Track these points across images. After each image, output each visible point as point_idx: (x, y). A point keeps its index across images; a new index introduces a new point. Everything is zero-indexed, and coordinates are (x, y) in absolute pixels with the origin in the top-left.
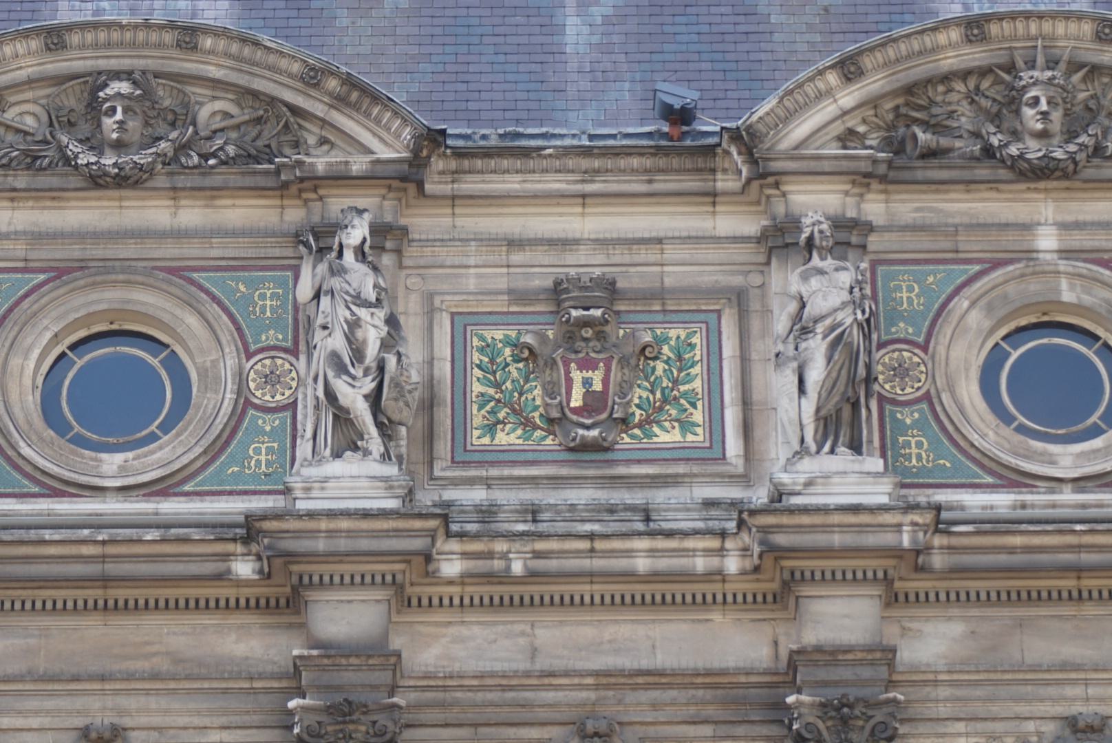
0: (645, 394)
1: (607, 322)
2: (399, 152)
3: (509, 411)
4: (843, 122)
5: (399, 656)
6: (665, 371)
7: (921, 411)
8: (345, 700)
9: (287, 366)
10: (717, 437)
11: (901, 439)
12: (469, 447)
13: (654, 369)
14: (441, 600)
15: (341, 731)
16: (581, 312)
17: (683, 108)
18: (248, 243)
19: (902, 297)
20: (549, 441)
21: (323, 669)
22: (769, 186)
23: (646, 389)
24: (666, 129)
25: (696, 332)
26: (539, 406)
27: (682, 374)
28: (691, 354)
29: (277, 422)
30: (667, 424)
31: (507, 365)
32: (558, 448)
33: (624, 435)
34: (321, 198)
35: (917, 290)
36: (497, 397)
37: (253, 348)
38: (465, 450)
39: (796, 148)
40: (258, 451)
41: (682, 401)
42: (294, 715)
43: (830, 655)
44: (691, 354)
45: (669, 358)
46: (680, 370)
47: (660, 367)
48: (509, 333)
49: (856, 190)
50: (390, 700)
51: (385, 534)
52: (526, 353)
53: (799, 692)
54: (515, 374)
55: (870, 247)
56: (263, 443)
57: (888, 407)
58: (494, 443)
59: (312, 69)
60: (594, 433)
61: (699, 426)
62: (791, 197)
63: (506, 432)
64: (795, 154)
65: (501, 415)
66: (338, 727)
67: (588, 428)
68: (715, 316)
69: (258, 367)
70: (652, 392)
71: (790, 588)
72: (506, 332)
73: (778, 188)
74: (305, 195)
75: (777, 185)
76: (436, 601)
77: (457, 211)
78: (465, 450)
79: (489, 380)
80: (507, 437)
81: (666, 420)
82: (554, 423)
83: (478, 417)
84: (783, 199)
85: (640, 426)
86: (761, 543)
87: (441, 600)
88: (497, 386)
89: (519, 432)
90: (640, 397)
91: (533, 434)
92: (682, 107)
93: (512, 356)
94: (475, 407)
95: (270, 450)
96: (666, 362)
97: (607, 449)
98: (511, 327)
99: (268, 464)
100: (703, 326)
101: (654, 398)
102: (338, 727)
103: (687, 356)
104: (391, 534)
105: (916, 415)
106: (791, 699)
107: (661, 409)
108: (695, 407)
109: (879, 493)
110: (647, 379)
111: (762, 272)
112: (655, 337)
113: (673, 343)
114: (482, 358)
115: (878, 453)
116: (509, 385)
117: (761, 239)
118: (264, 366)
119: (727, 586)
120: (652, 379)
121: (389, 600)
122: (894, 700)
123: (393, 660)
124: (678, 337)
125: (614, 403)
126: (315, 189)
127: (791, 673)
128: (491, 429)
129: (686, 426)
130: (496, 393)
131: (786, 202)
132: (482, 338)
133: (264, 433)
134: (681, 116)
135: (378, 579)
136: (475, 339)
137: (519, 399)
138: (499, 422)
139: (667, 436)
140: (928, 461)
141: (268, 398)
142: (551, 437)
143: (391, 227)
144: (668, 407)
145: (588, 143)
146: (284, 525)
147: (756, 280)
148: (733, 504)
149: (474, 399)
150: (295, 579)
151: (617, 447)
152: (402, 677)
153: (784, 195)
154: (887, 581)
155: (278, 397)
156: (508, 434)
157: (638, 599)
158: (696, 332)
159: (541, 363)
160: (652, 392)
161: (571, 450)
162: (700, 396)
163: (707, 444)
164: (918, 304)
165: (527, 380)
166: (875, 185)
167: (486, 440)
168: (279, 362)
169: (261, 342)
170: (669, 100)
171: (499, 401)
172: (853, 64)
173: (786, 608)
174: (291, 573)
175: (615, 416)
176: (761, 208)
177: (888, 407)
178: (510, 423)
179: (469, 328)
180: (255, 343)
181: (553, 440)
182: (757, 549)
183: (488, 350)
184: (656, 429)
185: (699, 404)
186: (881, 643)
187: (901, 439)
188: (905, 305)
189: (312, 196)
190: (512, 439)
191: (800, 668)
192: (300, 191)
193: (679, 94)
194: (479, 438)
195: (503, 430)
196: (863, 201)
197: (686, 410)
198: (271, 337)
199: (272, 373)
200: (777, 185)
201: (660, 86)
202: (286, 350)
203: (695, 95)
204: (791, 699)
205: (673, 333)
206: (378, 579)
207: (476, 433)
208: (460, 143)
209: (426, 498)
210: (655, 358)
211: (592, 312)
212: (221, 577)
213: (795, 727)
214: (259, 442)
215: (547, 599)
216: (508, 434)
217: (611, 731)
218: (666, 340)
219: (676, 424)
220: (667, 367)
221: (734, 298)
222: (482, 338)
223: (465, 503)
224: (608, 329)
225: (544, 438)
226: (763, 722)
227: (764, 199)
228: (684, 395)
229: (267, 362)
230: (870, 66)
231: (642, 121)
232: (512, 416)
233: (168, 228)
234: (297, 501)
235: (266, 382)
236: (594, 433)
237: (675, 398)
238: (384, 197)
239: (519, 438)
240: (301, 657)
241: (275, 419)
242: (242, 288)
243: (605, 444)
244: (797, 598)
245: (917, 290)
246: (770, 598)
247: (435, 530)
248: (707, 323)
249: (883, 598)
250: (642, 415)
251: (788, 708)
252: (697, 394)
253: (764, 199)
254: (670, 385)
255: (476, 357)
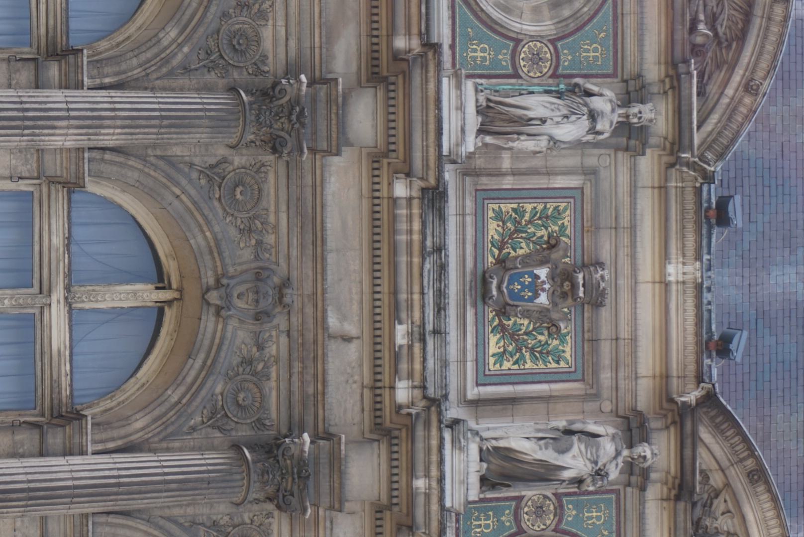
0: (524, 329)
1: (575, 300)
2: (698, 149)
3: (512, 230)
4: (716, 470)
5: (337, 155)
6: (540, 341)
7: (510, 527)
8: (310, 475)
9: (545, 70)
10: (494, 380)
11: (491, 513)
12: (486, 202)
13: (542, 334)
14: (378, 176)
15: (287, 472)
16: (581, 282)
17: (730, 350)
18: (634, 50)
19: (592, 512)
20: (491, 259)
21: (329, 101)
22: (673, 416)
23: (528, 327)
24: (716, 337)
25: (568, 364)
26: (516, 252)
27: (538, 355)
28: (551, 361)
29: (504, 63)
30: (502, 343)
31: (546, 228)
32: (486, 268)
33: (494, 313)
34: (665, 93)
35: (598, 523)
36: (523, 221)
37: (559, 44)
38: (484, 199)
39: (702, 440)
40: (483, 50)
41: (518, 354)
42: (299, 438)
43: (337, 464)
44: (551, 361)
45: (549, 345)
46: (540, 352)
47: (542, 338)
48: (568, 230)
49: (670, 480)
50: (306, 150)
51: (427, 510)
52: (553, 242)
53: (312, 442)
54: (539, 234)
55: (629, 490)
56: (489, 54)
57: (514, 503)
58: (490, 220)
59: (758, 86)
60: (495, 293)
61: (501, 367)
62: (665, 434)
63: (498, 228)
64: (695, 434)
65: (509, 225)
66: (290, 470)
67: (499, 288)
68: (580, 377)
69: (546, 49)
70: (526, 333)
71: (386, 436)
72: (569, 227)
73: (672, 423)
74: (667, 80)
75: (674, 422)
76: (376, 180)
77: (657, 285)
78: (484, 199)
79: (535, 215)
80: (493, 229)
81: (505, 342)
82: (501, 262)
83: (507, 207)
84: (664, 427)
85: (501, 324)
86: (418, 414)
87: (378, 176)
88: (530, 222)
89: (496, 237)
90: (521, 248)
91: (495, 248)
92: (731, 350)
93: (552, 231)
94: (515, 206)
95: (484, 58)
96: (546, 343)
97: (484, 303)
98: (573, 231)
99: (474, 59)
100: (573, 369)
101: (522, 335)
102: (290, 470)
103: (550, 358)
104: (425, 162)
105: (508, 524)
106: (306, 436)
107: (512, 336)
108: (514, 364)
109: (454, 498)
110: (534, 329)
111: (612, 411)
112: (565, 335)
113: (561, 348)
114: (551, 210)
115: (482, 496)
116: (532, 230)
117: (634, 410)
118: (546, 53)
119: (387, 390)
120: (534, 333)
121: (376, 147)
122: (304, 510)
123: (334, 151)
124: (564, 352)
125: (517, 306)
126: (672, 87)
127: (325, 436)
128: (499, 216)
129: (501, 357)
130: (526, 221)
131: (661, 429)
132: (565, 209)
133: (496, 55)
134: (723, 347)
135: (392, 140)
136: (564, 205)
137: (521, 237)
138: (504, 223)
139: (494, 344)
140: (476, 532)
141: (523, 55)
142: (494, 261)
143: (647, 479)
144: (514, 344)
145: (705, 286)
146: (431, 73)
147: (607, 406)
148: (446, 397)
149: (521, 205)
150: (392, 79)
151: (486, 308)
152: (323, 156)
153: (667, 428)
154: (390, 506)
155: (526, 517)
156: (496, 230)
157: (378, 318)
158: (568, 364)
159: (547, 252)
160: (526, 333)
161: (484, 273)
162: (522, 367)
163: (487, 372)
164: (587, 524)
165: (534, 243)
166: (673, 492)
167: (491, 214)
168: (548, 64)
169: (567, 505)
170: (735, 341)
171: (519, 223)
172: (759, 477)
173: (371, 432)
174: (396, 76)
175: (508, 308)
176: (658, 410)
177: (514, 503)
178: (504, 230)
179: (572, 200)
180: (566, 501)
181: (491, 263)
182: (413, 411)
183: (556, 214)
184: (498, 336)
185: (516, 367)
186: (347, 501)
187: (491, 513)
188: (586, 514)
189: (667, 86)
190: (492, 232)
191: (328, 442)
192: (671, 77)
193: (739, 345)
194: (493, 209)
195: (498, 226)
196: (662, 484)
197: (512, 357)
198: (566, 58)
199: (541, 59)
200: (674, 422)
201: (745, 334)
202: (557, 67)
203: (738, 359)
204: (306, 436)
205: (568, 349)
206: (392, 140)
207: (496, 207)
208: (705, 194)
209: (449, 175)
210: (550, 335)
211: (582, 289)
212: (396, 318)
213: (287, 440)
214: (490, 50)
215: (377, 274)
216: (496, 230)
217: (284, 306)
218: (563, 342)
219: (502, 350)
220: (543, 343)
221: (593, 391)
222: (565, 209)
223: (447, 320)
224: (570, 301)
225: (494, 256)
226: (290, 417)
227: (663, 412)
228: (522, 357)
229: (548, 55)
230: (759, 489)
231: (720, 323)
232: (509, 232)
233: (646, 499)
234: (447, 79)
235: (534, 54)
236: (495, 293)
237: (521, 350)
238: (666, 138)
239: (492, 237)
240: (340, 439)
241: (506, 61)
242: (602, 35)
243: (487, 300)
244: (378, 441)
245: (598, 523)
246: (379, 420)
247: (427, 180)
248: (575, 372)
249: (378, 502)
250: (509, 326)
251: (300, 436)
252: (524, 365)
253: (663, 412)
254: (530, 346)
255: (551, 206)
